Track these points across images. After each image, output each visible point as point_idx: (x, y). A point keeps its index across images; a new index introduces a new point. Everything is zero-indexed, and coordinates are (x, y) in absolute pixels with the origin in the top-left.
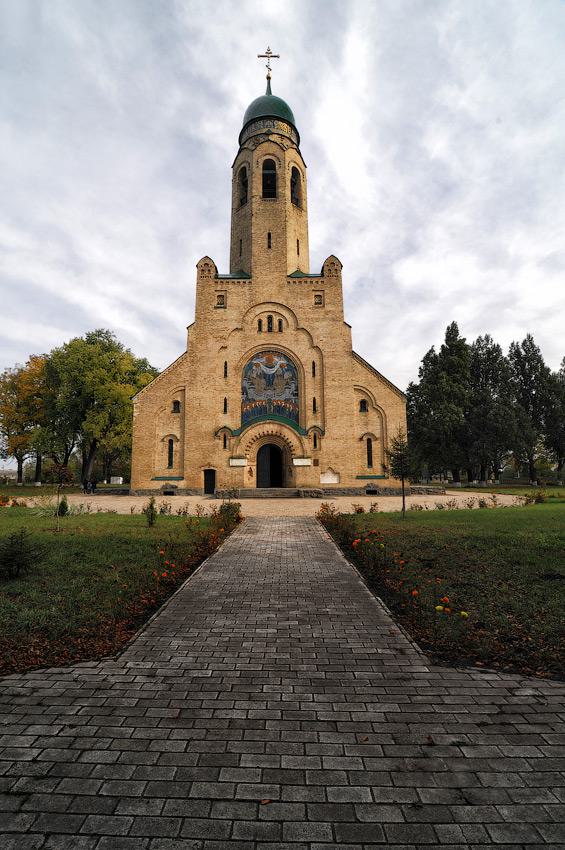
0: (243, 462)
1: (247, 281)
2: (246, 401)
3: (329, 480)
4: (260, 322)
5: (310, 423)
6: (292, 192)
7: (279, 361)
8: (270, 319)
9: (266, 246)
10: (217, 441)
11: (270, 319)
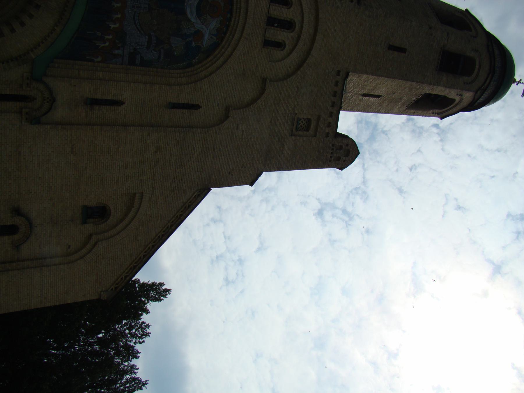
7: (209, 29)
8: (288, 25)
11: (288, 25)
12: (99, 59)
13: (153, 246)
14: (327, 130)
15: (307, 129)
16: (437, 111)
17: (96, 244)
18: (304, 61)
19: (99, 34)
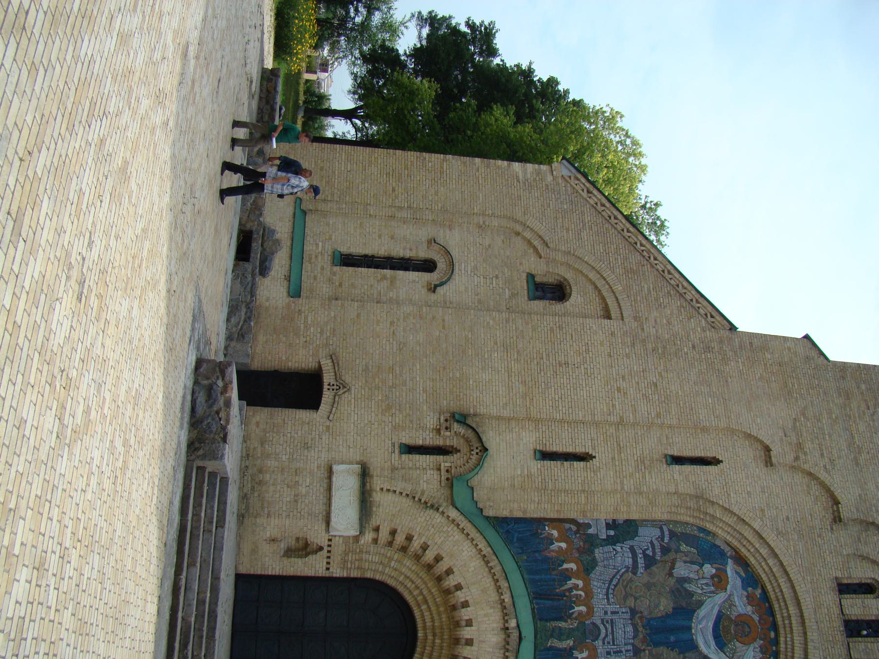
10: (431, 421)
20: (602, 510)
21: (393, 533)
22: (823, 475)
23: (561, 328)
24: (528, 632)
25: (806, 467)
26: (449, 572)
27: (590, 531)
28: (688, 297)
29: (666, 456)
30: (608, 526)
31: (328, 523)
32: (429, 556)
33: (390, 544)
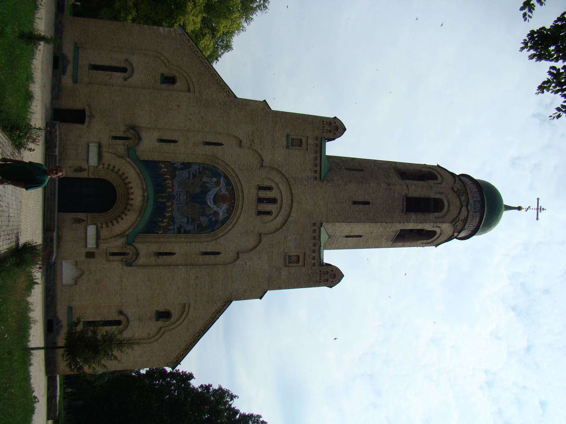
0: (93, 160)
1: (318, 175)
2: (172, 167)
3: (67, 272)
4: (270, 189)
5: (143, 248)
6: (411, 231)
8: (273, 201)
9: (356, 199)
10: (122, 128)
11: (273, 201)
12: (161, 232)
13: (199, 336)
14: (313, 261)
15: (298, 263)
16: (425, 241)
17: (164, 333)
18: (287, 220)
19: (160, 219)
20: (181, 158)
21: (109, 165)
22: (260, 151)
23: (171, 95)
24: (152, 197)
25: (254, 148)
26: (127, 178)
27: (175, 165)
28: (221, 84)
29: (203, 142)
30: (182, 164)
31: (88, 161)
32: (120, 173)
33: (108, 169)
